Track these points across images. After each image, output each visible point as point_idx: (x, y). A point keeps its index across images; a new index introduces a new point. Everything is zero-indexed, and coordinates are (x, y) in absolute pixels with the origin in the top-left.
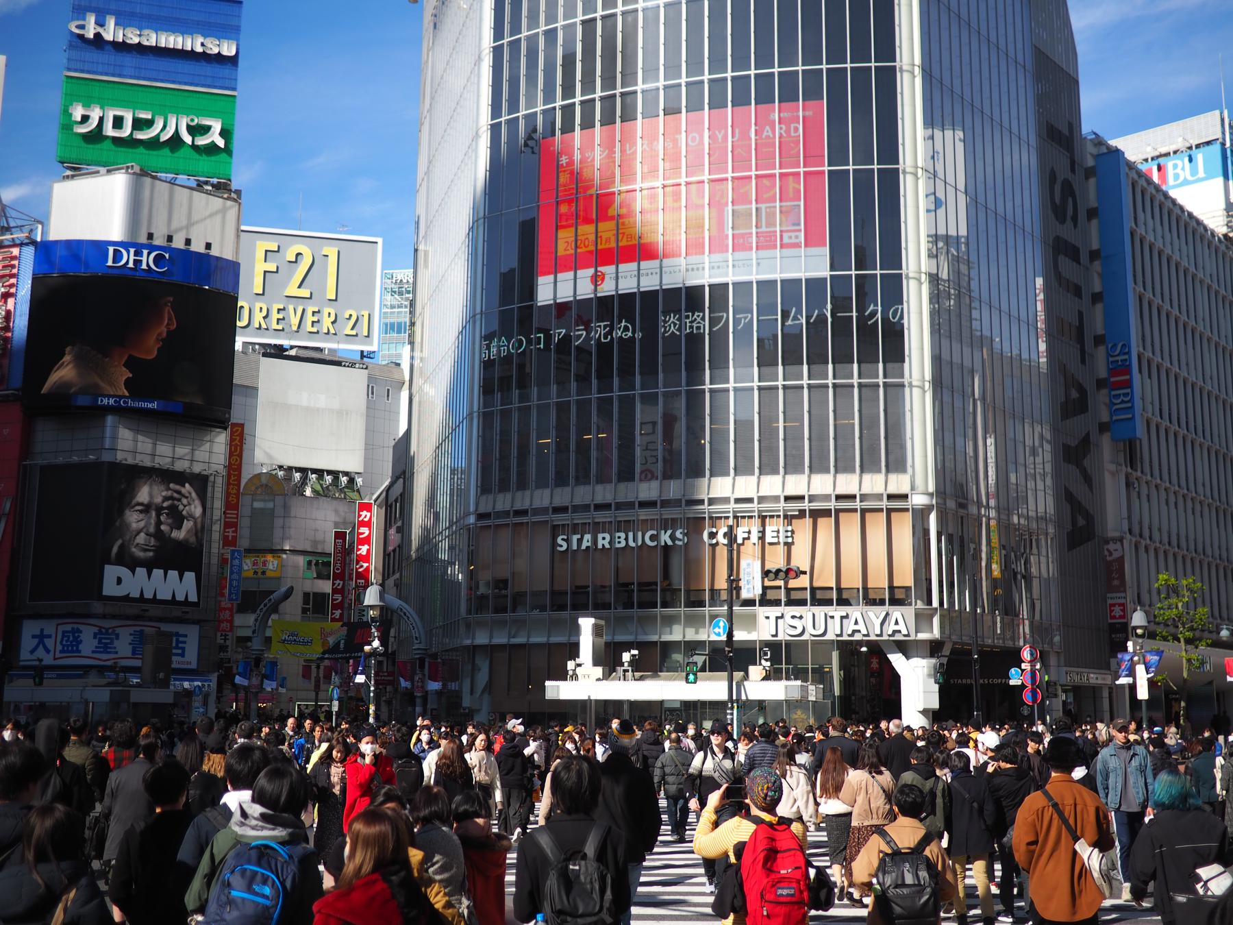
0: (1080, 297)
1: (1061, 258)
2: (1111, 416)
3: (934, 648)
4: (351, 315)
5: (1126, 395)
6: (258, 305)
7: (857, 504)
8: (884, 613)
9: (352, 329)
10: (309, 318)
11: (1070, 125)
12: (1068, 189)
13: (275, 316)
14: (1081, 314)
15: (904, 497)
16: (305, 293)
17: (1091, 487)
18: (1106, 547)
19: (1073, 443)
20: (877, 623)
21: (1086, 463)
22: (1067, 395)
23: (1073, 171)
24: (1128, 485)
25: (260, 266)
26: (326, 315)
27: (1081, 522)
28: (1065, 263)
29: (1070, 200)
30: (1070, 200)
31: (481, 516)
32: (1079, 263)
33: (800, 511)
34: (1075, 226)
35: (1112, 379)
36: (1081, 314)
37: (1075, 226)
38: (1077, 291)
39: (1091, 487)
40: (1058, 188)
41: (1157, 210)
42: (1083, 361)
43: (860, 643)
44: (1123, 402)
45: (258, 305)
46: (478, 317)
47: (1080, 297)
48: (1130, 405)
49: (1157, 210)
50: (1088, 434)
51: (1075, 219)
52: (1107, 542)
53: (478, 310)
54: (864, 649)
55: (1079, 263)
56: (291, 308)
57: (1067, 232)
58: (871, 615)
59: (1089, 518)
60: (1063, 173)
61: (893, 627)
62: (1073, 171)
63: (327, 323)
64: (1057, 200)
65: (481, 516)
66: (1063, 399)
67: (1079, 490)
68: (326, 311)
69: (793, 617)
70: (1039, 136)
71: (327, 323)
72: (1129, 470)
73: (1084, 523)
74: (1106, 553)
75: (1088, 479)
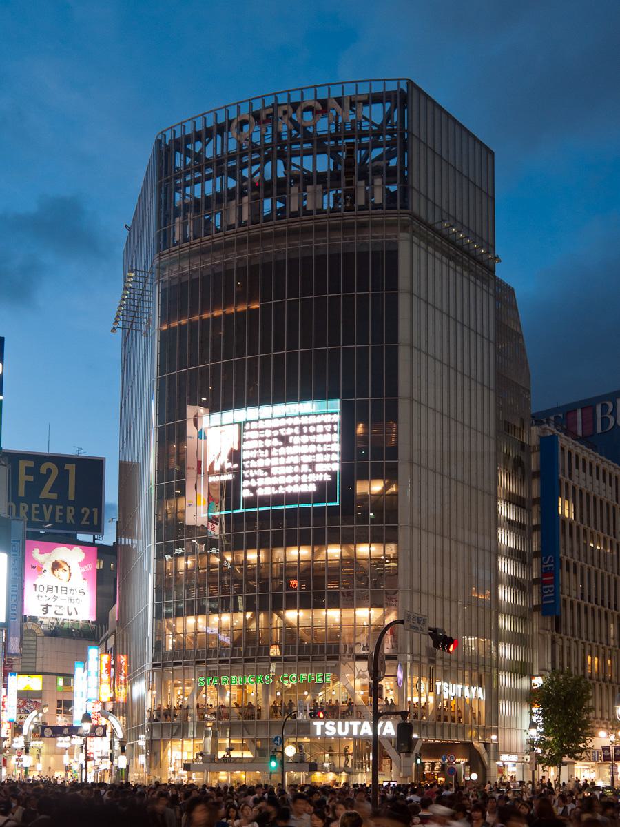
2: (542, 601)
4: (85, 511)
5: (551, 589)
6: (22, 505)
9: (87, 521)
10: (58, 514)
16: (54, 496)
26: (68, 511)
35: (544, 579)
41: (587, 467)
44: (549, 593)
45: (22, 505)
48: (552, 595)
49: (587, 467)
56: (44, 506)
63: (70, 517)
68: (69, 508)
71: (70, 517)
72: (555, 633)
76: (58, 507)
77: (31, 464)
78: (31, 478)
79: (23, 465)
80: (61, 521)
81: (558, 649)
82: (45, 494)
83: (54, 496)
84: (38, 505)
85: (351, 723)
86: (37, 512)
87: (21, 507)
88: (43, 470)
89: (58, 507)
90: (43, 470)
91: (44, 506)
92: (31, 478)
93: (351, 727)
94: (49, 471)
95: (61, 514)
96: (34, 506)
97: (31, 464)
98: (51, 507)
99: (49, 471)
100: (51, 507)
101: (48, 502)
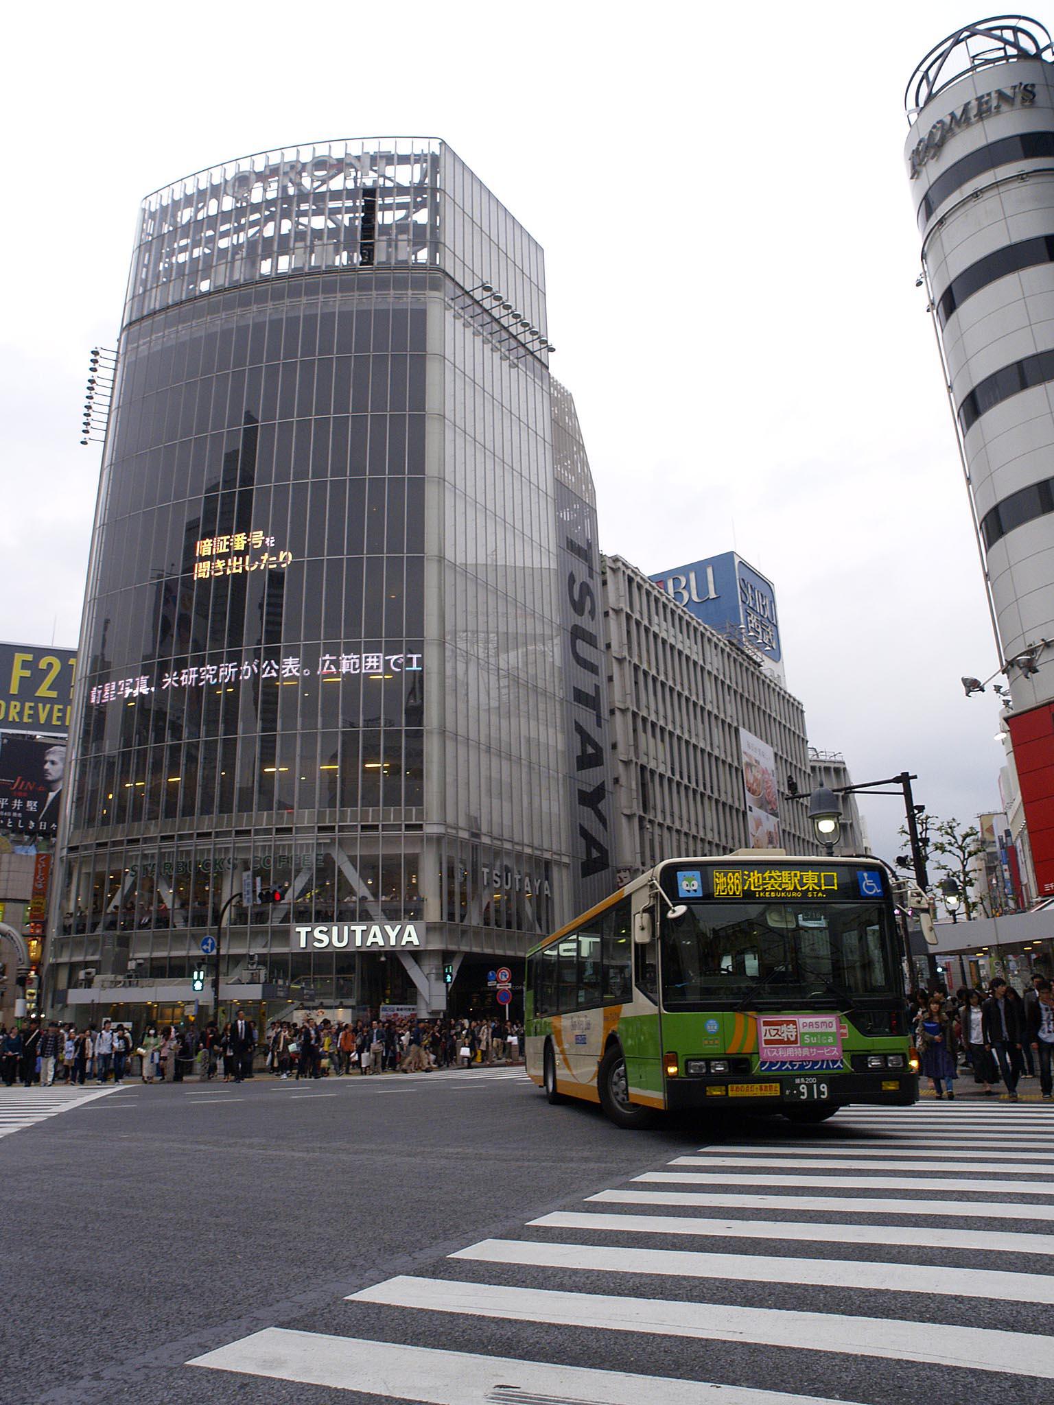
0: (597, 674)
1: (579, 642)
3: (447, 956)
6: (13, 703)
7: (380, 832)
8: (398, 927)
10: (56, 714)
11: (589, 545)
12: (586, 590)
13: (27, 712)
14: (597, 687)
15: (420, 827)
16: (54, 694)
17: (605, 824)
18: (618, 875)
19: (589, 789)
20: (393, 935)
21: (600, 806)
22: (584, 750)
23: (591, 576)
24: (641, 827)
25: (18, 673)
27: (595, 854)
28: (583, 648)
29: (588, 598)
30: (588, 598)
31: (72, 849)
32: (597, 648)
33: (331, 838)
34: (593, 619)
36: (597, 687)
37: (593, 619)
38: (593, 669)
39: (605, 824)
40: (576, 588)
42: (599, 725)
43: (379, 953)
45: (13, 703)
46: (83, 679)
47: (597, 674)
50: (604, 782)
51: (592, 613)
52: (619, 872)
53: (84, 675)
54: (383, 959)
55: (597, 648)
56: (40, 705)
57: (584, 622)
58: (388, 928)
59: (604, 852)
60: (581, 576)
61: (405, 939)
62: (591, 576)
64: (576, 597)
65: (72, 849)
66: (580, 754)
67: (594, 827)
69: (321, 932)
70: (559, 546)
73: (599, 855)
74: (619, 880)
75: (602, 820)
76: (56, 707)
77: (29, 657)
78: (27, 673)
79: (19, 658)
80: (59, 723)
81: (647, 837)
82: (43, 691)
83: (54, 694)
84: (32, 704)
85: (353, 928)
86: (31, 712)
87: (12, 707)
88: (43, 664)
89: (56, 707)
90: (43, 664)
91: (40, 705)
92: (27, 673)
93: (352, 933)
94: (50, 665)
95: (60, 715)
96: (28, 705)
97: (29, 657)
98: (48, 706)
99: (50, 665)
100: (48, 706)
101: (45, 700)
